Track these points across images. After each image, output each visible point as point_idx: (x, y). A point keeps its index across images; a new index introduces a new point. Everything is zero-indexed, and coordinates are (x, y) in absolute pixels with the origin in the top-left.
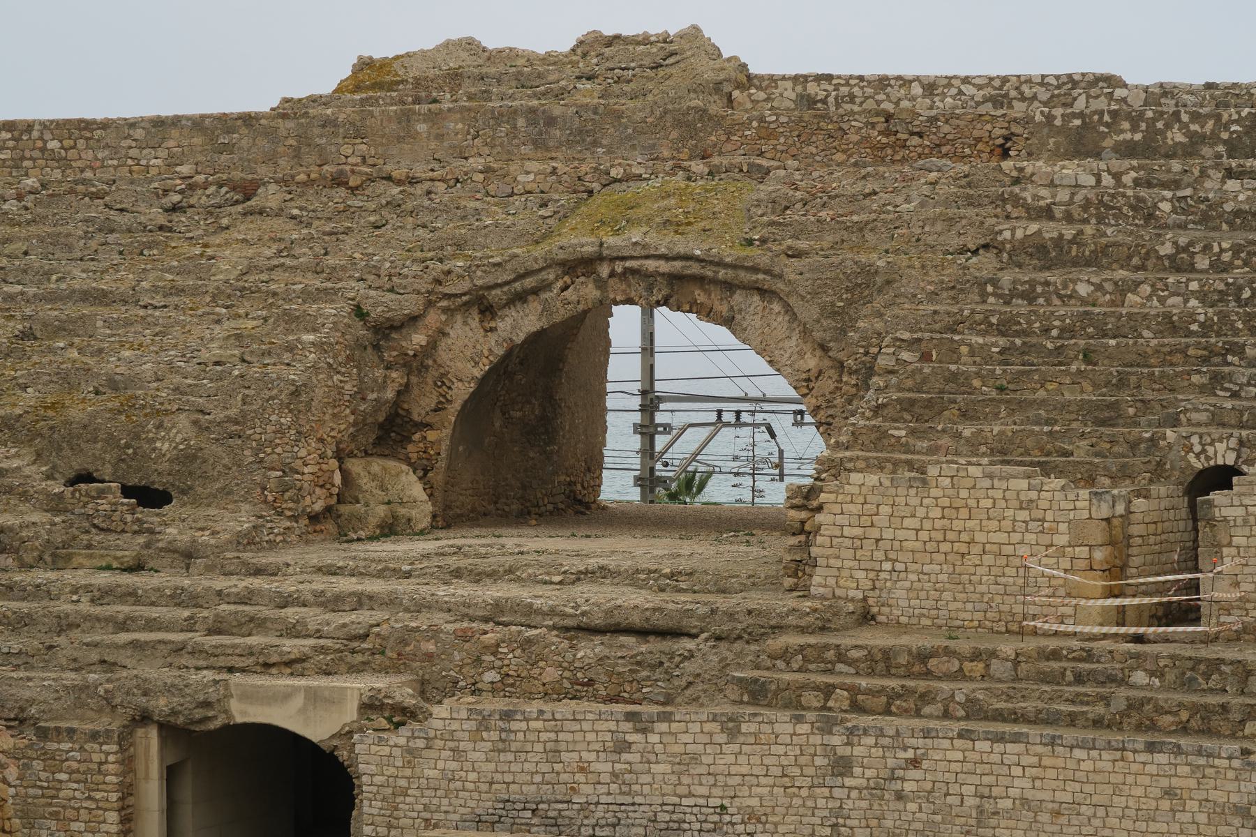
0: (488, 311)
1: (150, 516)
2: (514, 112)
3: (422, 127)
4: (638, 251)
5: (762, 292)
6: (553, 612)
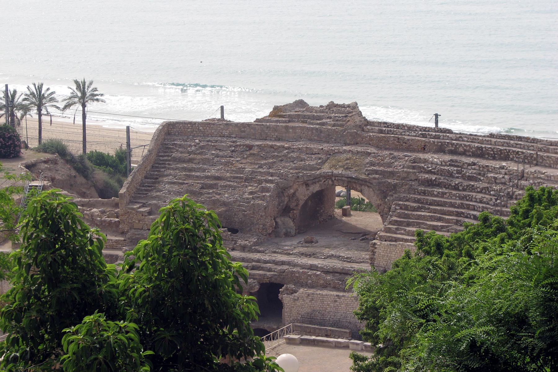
0: (307, 185)
1: (234, 237)
2: (313, 129)
3: (291, 130)
4: (341, 176)
5: (368, 186)
6: (322, 268)
